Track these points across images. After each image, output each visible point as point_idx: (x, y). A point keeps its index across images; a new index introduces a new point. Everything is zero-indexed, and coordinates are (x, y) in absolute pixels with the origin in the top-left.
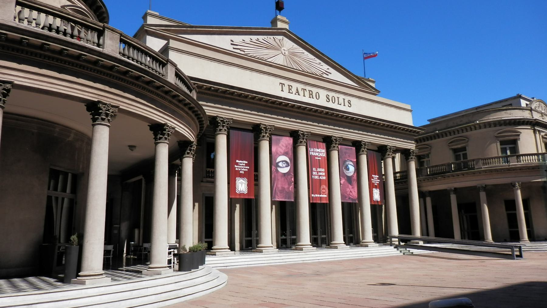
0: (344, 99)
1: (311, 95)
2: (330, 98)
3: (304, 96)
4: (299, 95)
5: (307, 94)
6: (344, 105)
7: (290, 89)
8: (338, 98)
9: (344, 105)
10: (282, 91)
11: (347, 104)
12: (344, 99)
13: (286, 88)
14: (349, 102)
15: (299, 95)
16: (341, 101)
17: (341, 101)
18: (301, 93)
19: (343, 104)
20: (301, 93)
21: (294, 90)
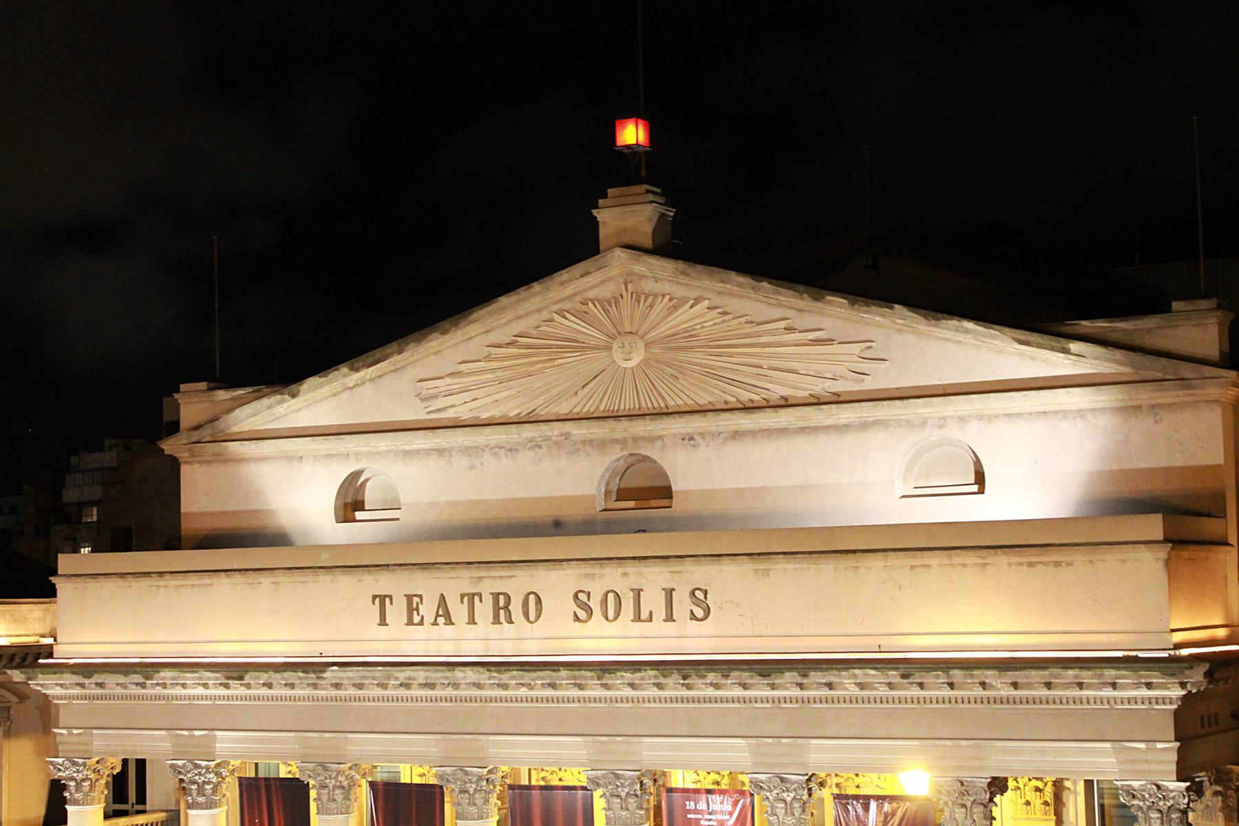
0: (669, 593)
1: (501, 608)
2: (595, 604)
3: (472, 621)
4: (449, 622)
5: (484, 609)
6: (670, 618)
7: (411, 609)
8: (638, 593)
9: (670, 618)
10: (383, 622)
11: (682, 605)
12: (669, 593)
13: (396, 612)
14: (699, 597)
15: (449, 622)
16: (653, 601)
17: (653, 601)
18: (459, 611)
19: (660, 613)
20: (459, 611)
21: (428, 609)
